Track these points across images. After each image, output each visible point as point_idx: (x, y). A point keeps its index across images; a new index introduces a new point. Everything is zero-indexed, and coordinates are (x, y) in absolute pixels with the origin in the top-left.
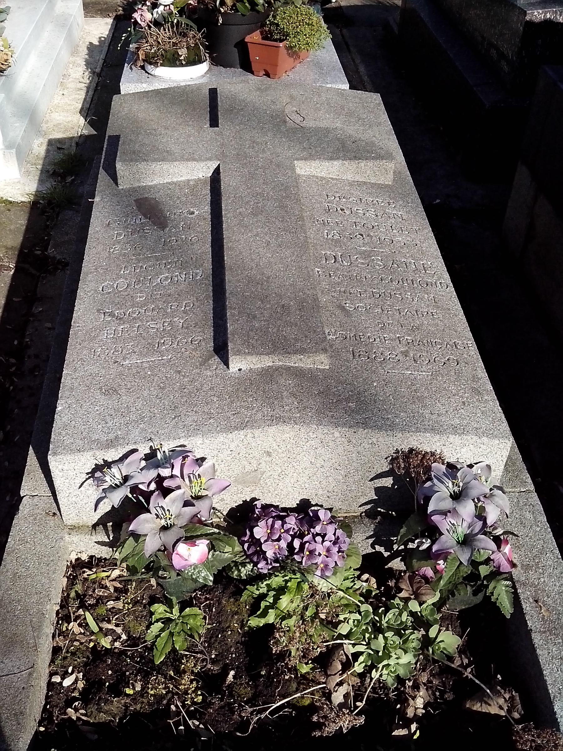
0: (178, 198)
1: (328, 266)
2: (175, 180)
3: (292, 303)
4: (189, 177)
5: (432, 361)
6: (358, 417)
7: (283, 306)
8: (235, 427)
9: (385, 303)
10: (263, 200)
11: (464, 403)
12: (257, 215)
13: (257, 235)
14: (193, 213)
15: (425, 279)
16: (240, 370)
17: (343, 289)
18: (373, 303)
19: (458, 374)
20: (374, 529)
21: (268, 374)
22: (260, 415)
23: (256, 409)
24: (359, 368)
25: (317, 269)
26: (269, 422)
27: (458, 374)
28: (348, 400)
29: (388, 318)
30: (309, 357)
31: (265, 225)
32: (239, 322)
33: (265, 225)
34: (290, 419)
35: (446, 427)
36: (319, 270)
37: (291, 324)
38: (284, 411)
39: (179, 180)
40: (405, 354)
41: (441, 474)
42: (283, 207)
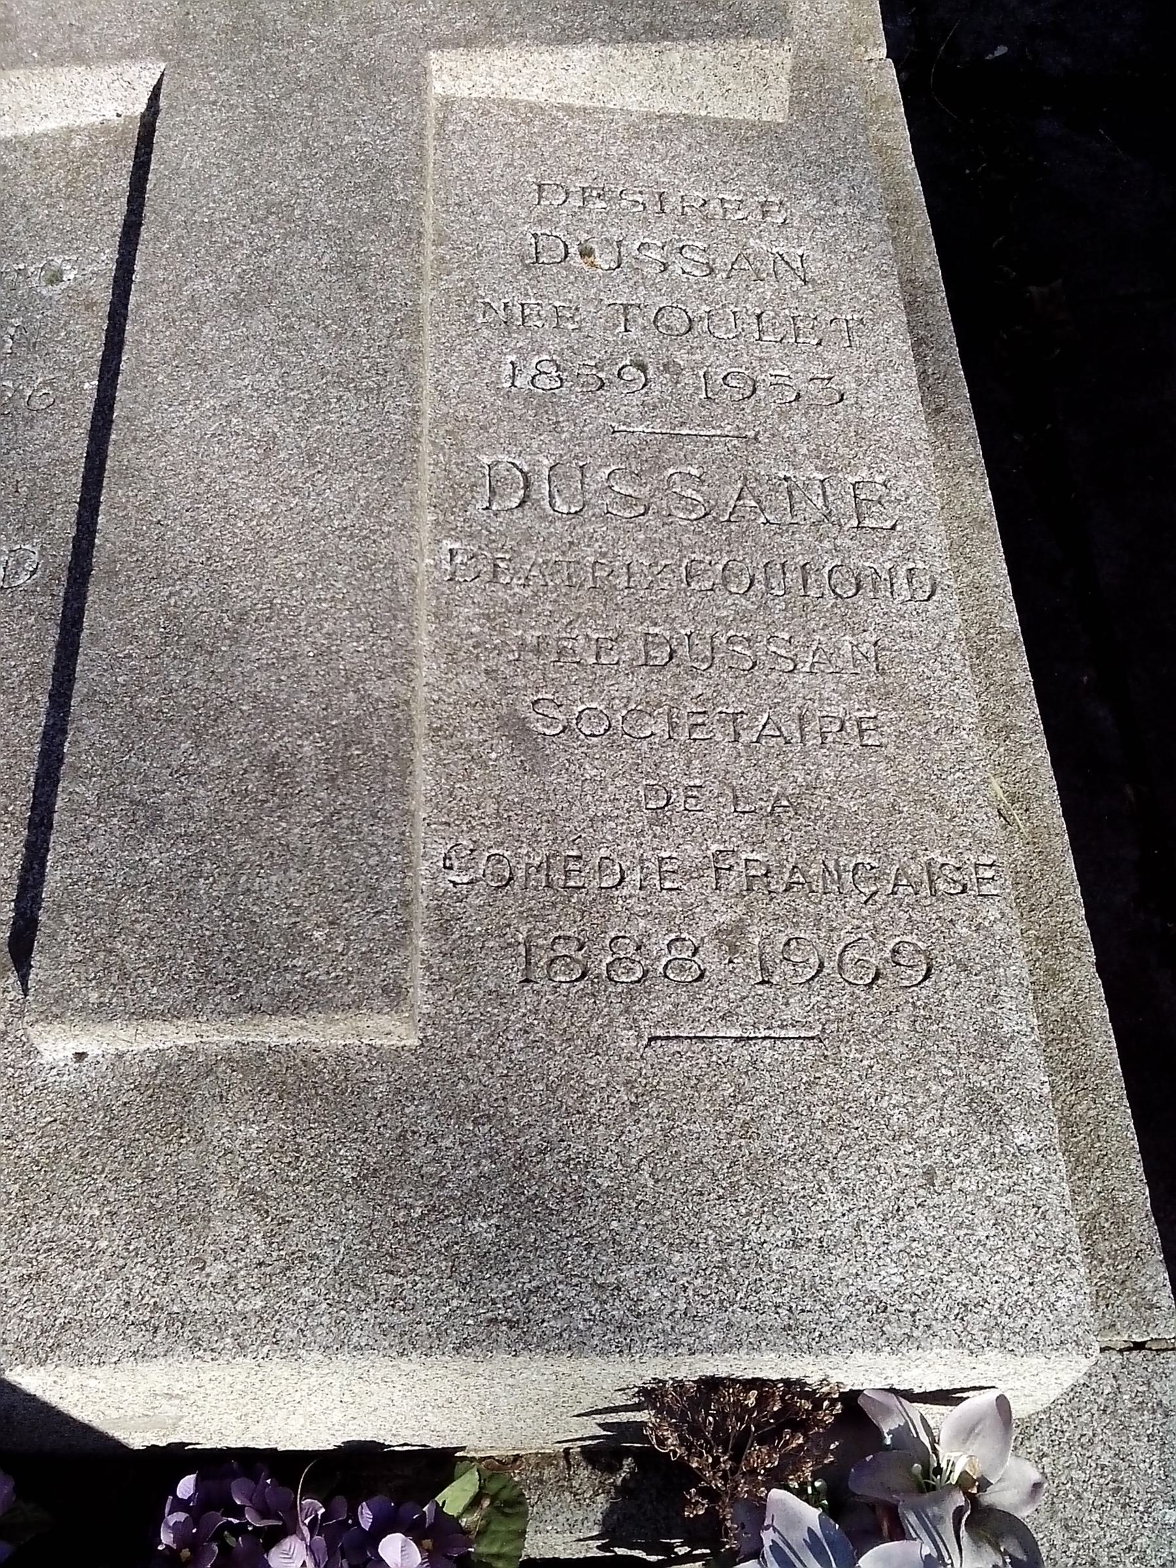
0: (25, 208)
1: (494, 525)
2: (25, 130)
3: (308, 750)
4: (71, 119)
5: (830, 965)
6: (499, 1289)
7: (272, 762)
8: (18, 1344)
9: (685, 691)
10: (285, 237)
11: (930, 1174)
12: (251, 311)
13: (232, 408)
14: (56, 278)
15: (854, 561)
16: (80, 1056)
17: (531, 637)
18: (637, 695)
19: (925, 1020)
20: (607, 1515)
21: (171, 1090)
22: (113, 1292)
23: (105, 1263)
24: (540, 1030)
25: (448, 544)
26: (138, 1338)
27: (925, 1020)
28: (470, 1202)
29: (689, 763)
30: (332, 1022)
31: (274, 356)
32: (91, 847)
33: (274, 356)
34: (221, 1328)
35: (843, 1313)
36: (456, 546)
37: (286, 856)
38: (201, 1287)
39: (38, 130)
40: (731, 939)
41: (798, 1537)
42: (350, 268)
